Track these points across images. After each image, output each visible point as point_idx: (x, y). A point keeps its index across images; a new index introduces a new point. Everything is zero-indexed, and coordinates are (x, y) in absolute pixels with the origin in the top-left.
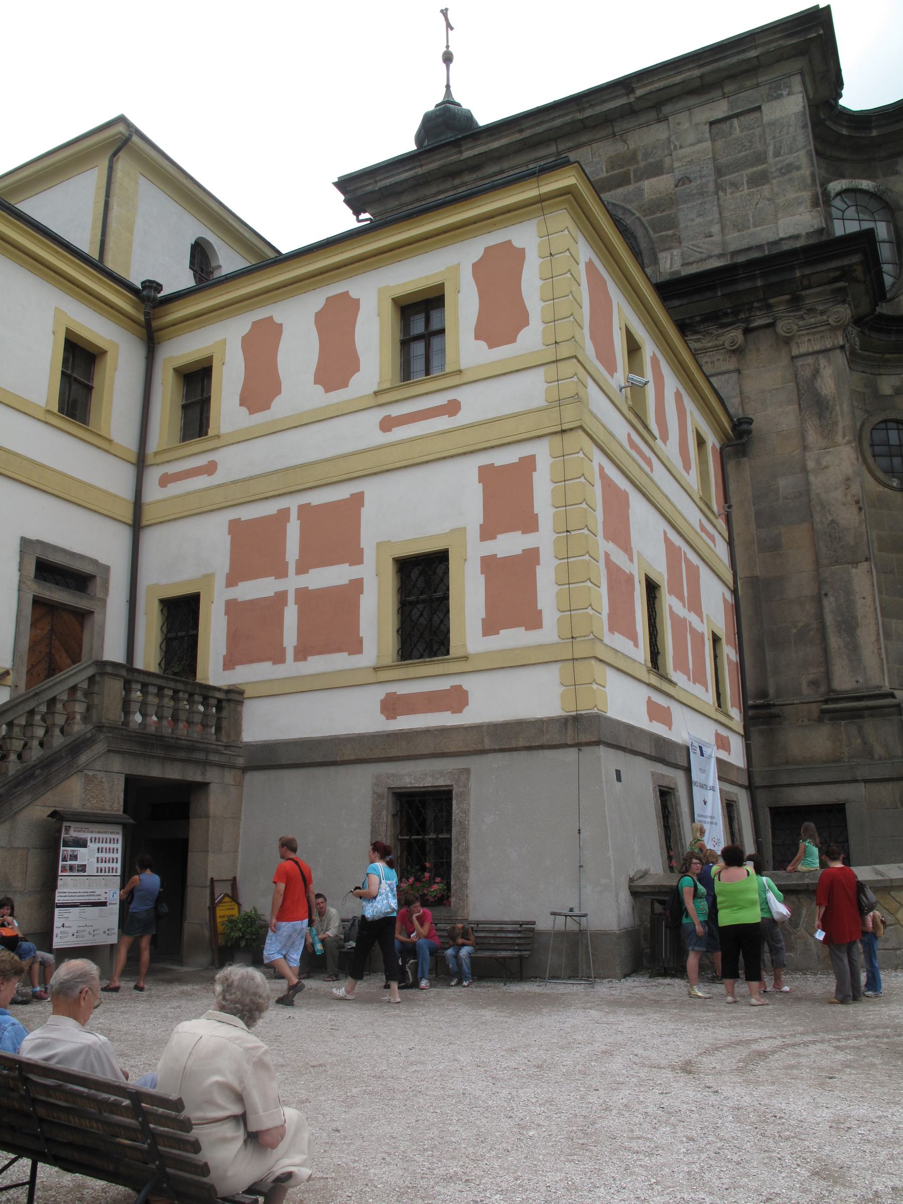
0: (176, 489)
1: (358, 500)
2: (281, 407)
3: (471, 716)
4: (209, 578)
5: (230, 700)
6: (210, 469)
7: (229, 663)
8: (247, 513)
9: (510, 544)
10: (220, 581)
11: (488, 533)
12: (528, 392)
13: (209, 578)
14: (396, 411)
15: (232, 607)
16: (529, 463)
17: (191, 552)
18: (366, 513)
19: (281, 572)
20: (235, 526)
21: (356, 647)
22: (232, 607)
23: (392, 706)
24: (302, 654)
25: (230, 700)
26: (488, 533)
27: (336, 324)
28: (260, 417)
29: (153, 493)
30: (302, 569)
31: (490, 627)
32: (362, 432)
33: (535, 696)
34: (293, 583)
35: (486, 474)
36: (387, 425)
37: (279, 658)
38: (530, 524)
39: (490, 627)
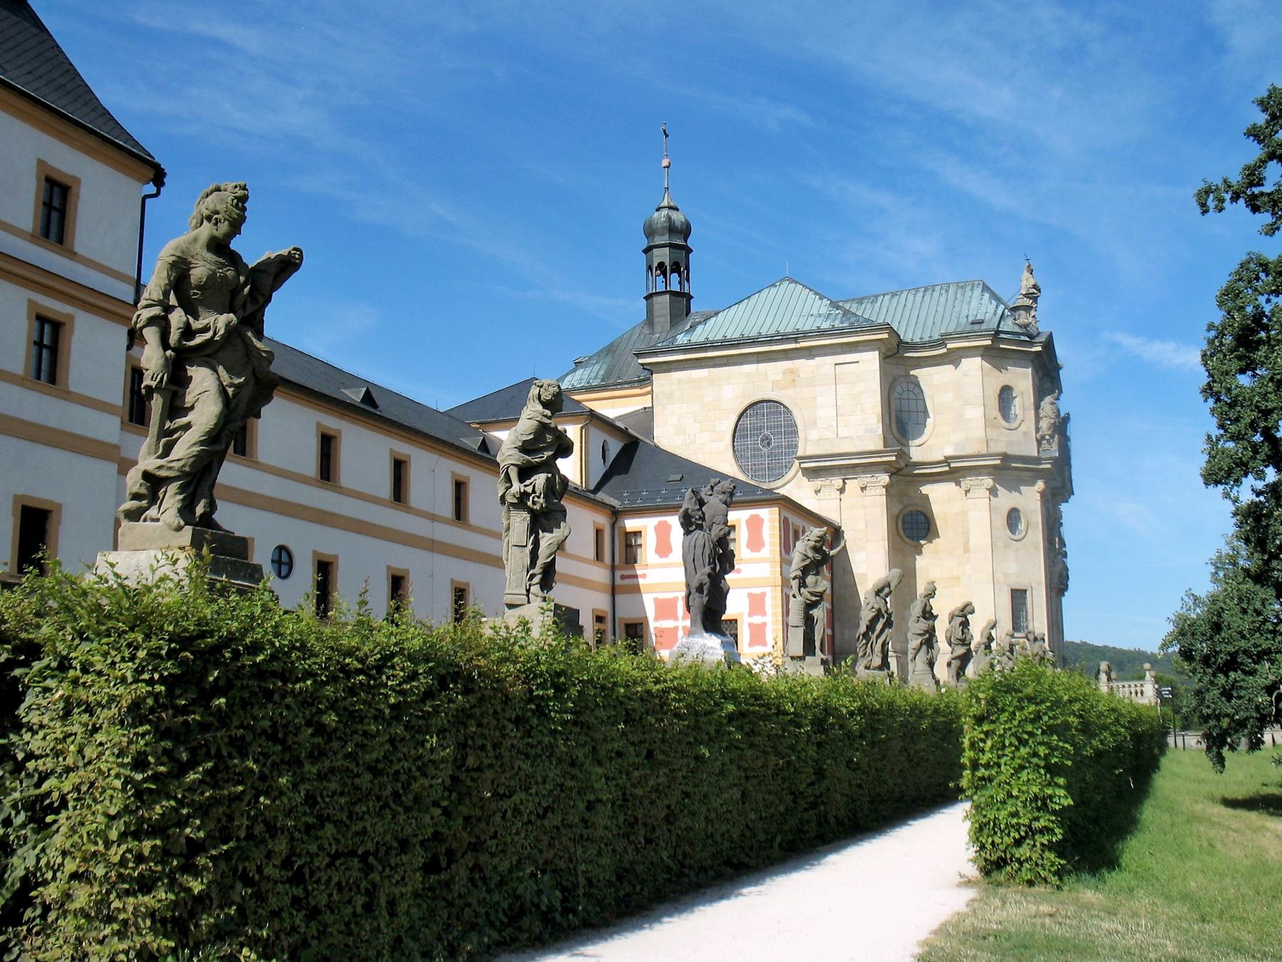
0: (627, 582)
8: (662, 596)
9: (757, 620)
11: (751, 614)
16: (763, 595)
26: (751, 614)
28: (664, 560)
29: (618, 581)
35: (750, 595)
38: (764, 614)
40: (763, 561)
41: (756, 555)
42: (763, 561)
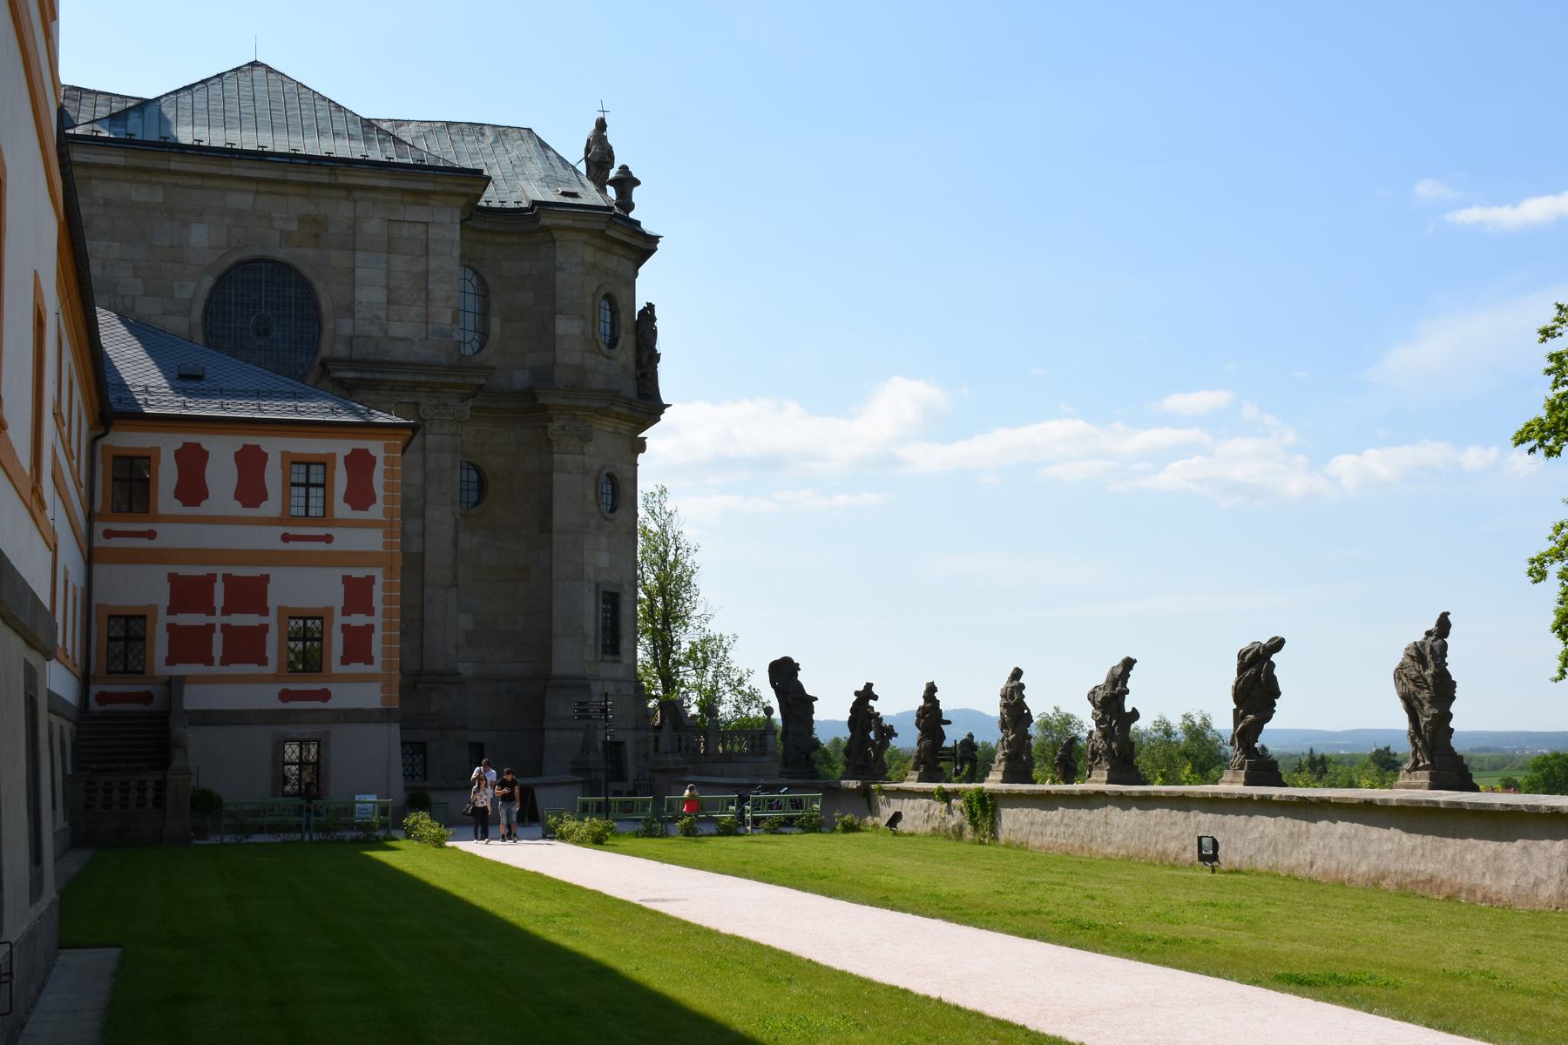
1: (265, 579)
2: (205, 508)
3: (332, 704)
4: (154, 608)
5: (174, 686)
6: (151, 535)
7: (170, 661)
9: (358, 620)
10: (162, 611)
11: (346, 611)
12: (372, 541)
13: (154, 608)
14: (293, 531)
15: (171, 628)
16: (370, 580)
17: (143, 589)
18: (271, 587)
19: (211, 611)
20: (173, 578)
21: (263, 661)
22: (171, 628)
23: (285, 696)
24: (224, 662)
25: (174, 686)
26: (346, 611)
27: (250, 462)
30: (225, 612)
31: (345, 660)
32: (270, 538)
33: (370, 696)
34: (218, 620)
36: (286, 538)
37: (209, 661)
38: (370, 611)
39: (345, 660)
40: (372, 524)
41: (359, 515)
42: (372, 524)
